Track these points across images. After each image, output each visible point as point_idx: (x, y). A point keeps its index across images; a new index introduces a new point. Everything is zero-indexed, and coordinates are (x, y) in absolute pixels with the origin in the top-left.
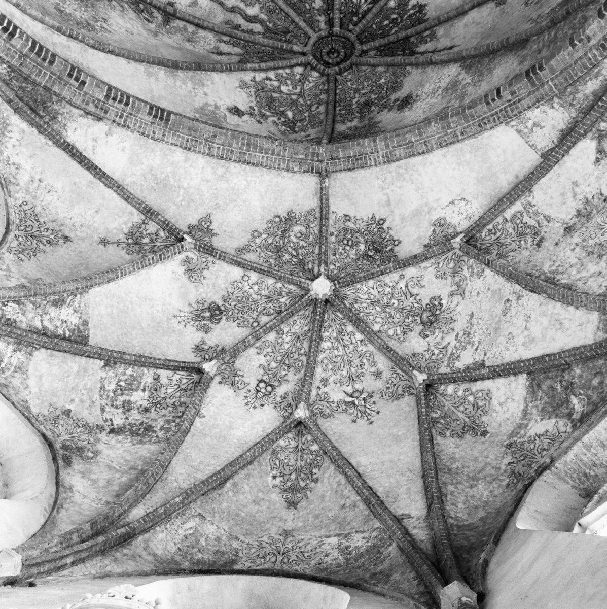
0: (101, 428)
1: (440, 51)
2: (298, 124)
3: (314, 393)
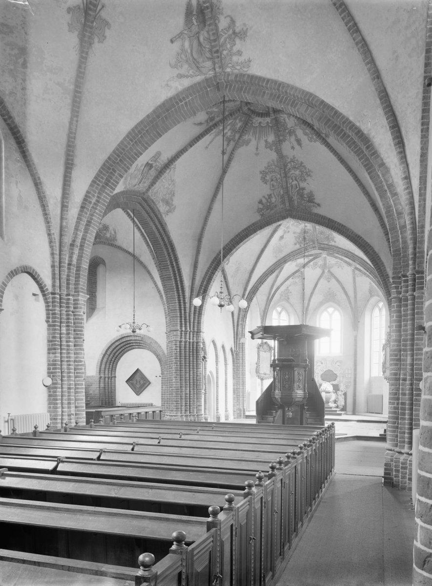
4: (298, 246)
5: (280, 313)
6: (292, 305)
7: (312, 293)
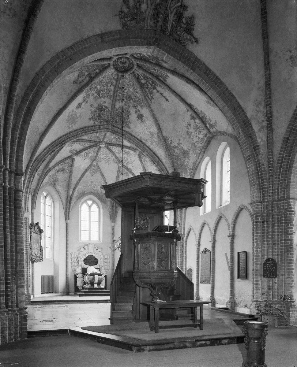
0: (56, 173)
1: (163, 97)
2: (102, 92)
3: (98, 157)
4: (91, 123)
5: (46, 197)
6: (58, 192)
7: (78, 183)
